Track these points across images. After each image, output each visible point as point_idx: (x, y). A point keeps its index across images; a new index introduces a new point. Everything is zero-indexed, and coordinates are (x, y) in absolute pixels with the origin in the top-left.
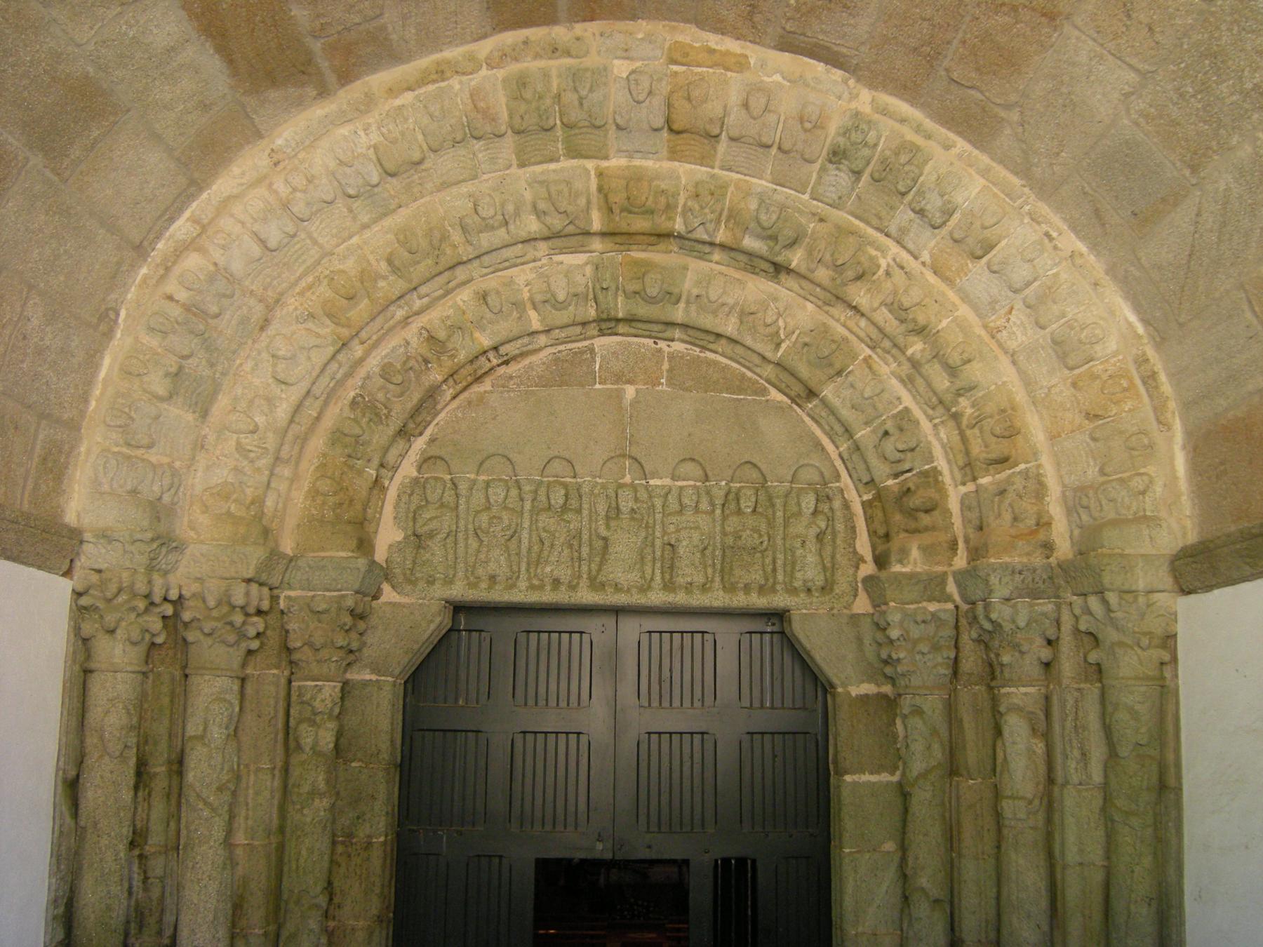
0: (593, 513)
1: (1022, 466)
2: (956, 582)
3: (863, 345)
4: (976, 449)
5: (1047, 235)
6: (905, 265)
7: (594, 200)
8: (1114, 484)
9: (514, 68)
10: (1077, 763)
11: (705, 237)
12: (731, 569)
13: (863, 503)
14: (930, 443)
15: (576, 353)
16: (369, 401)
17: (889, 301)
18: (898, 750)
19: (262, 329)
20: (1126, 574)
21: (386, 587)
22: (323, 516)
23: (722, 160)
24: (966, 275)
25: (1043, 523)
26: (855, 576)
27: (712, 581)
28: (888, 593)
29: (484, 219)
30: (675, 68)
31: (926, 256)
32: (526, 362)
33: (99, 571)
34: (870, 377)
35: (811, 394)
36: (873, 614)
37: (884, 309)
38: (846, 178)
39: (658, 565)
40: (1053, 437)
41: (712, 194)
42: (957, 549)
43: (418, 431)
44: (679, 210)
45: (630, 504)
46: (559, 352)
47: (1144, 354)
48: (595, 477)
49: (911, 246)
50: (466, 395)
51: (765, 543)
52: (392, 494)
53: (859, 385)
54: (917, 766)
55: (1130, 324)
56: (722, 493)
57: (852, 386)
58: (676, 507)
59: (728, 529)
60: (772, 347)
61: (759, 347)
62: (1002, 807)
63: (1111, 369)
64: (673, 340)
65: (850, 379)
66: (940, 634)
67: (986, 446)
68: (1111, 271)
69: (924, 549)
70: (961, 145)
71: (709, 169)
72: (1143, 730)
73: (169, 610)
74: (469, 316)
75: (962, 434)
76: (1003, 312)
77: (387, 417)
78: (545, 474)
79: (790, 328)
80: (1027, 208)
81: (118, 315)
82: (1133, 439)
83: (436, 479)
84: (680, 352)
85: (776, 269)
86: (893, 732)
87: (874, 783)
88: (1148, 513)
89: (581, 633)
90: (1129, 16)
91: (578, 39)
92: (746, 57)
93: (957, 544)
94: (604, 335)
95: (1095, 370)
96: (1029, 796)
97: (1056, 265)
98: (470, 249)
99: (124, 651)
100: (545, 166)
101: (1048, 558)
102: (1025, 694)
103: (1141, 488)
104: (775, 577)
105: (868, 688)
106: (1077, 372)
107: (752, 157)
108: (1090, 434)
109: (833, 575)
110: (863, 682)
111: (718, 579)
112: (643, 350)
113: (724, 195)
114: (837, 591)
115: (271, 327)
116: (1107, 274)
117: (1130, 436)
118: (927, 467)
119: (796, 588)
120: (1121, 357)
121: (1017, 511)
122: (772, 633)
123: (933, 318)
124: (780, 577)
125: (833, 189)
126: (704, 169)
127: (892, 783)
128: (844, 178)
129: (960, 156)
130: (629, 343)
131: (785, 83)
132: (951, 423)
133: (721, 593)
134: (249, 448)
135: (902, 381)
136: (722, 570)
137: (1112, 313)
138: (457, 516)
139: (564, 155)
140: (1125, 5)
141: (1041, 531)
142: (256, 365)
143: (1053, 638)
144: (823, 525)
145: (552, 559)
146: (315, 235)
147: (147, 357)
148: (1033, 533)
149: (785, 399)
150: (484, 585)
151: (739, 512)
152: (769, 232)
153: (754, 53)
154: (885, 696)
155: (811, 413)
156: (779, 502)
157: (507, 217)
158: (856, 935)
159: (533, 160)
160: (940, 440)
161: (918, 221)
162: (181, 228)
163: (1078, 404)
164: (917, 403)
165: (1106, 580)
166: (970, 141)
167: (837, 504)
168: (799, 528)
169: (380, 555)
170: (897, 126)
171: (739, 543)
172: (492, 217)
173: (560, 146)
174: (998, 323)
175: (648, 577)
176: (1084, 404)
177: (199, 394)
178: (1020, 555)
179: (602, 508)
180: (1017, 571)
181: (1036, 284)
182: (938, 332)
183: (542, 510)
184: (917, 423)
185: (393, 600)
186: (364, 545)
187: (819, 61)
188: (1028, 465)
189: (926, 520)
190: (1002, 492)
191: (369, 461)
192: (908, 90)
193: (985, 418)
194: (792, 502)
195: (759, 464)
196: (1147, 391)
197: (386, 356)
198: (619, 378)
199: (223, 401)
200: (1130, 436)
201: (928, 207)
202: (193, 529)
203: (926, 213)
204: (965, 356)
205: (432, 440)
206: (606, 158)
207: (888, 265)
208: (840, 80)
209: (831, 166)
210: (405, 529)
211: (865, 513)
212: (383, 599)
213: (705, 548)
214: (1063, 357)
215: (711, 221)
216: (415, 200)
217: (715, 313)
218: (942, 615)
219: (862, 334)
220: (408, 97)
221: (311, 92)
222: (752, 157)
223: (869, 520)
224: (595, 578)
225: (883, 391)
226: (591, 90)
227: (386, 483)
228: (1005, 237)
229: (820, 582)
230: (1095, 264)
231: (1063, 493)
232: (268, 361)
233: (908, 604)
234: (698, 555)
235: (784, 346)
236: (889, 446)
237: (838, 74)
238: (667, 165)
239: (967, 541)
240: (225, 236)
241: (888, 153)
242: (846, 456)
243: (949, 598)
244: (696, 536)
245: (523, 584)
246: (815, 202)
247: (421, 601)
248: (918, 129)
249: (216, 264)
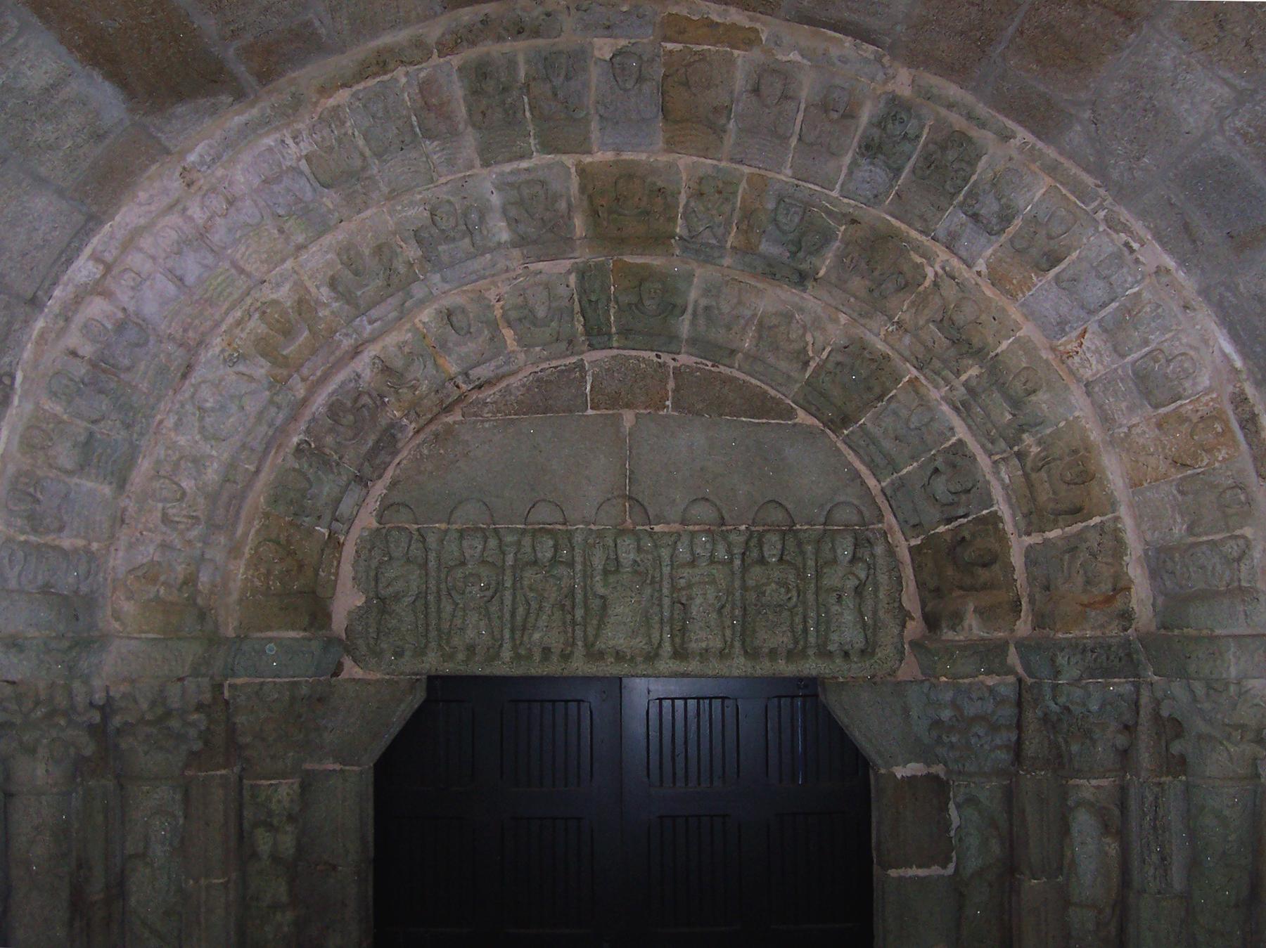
0: (587, 562)
1: (1097, 520)
3: (908, 365)
4: (1044, 496)
5: (1127, 244)
6: (957, 274)
8: (1204, 548)
9: (470, 54)
10: (1156, 869)
12: (754, 631)
13: (910, 549)
14: (988, 482)
15: (562, 371)
16: (316, 448)
17: (938, 317)
19: (184, 376)
20: (1215, 661)
21: (348, 662)
22: (269, 588)
24: (1030, 289)
25: (1121, 587)
26: (901, 635)
27: (732, 646)
29: (443, 231)
30: (670, 46)
31: (981, 265)
32: (503, 384)
33: (13, 683)
34: (916, 404)
35: (846, 421)
36: (922, 682)
37: (931, 325)
38: (883, 174)
39: (667, 629)
40: (1135, 485)
41: (720, 192)
43: (376, 474)
44: (681, 210)
45: (632, 556)
47: (1242, 392)
48: (588, 524)
49: (964, 254)
50: (433, 427)
51: (795, 599)
52: (349, 551)
53: (904, 413)
54: (973, 864)
55: (1225, 356)
56: (742, 539)
57: (895, 413)
58: (688, 557)
59: (751, 583)
61: (783, 365)
63: (1203, 410)
64: (678, 354)
65: (893, 405)
67: (1054, 493)
68: (1204, 292)
69: (979, 611)
70: (1023, 134)
71: (715, 162)
72: (1232, 837)
73: (97, 717)
75: (1026, 475)
76: (1075, 334)
77: (338, 464)
78: (528, 520)
79: (819, 345)
80: (1101, 214)
81: (13, 378)
82: (1229, 493)
83: (399, 529)
84: (688, 367)
85: (800, 274)
87: (925, 877)
88: (1244, 584)
89: (579, 701)
90: (1221, 28)
91: (548, 15)
92: (756, 31)
94: (595, 349)
95: (1183, 410)
97: (1137, 282)
99: (47, 771)
100: (515, 165)
101: (1125, 629)
102: (1098, 787)
103: (1235, 555)
104: (806, 639)
105: (914, 768)
106: (1162, 411)
108: (1178, 485)
109: (875, 635)
111: (737, 644)
113: (735, 193)
115: (195, 374)
116: (1199, 293)
117: (1224, 491)
118: (985, 512)
119: (831, 652)
120: (1214, 396)
121: (1090, 574)
122: (804, 696)
123: (990, 340)
124: (812, 640)
125: (867, 186)
126: (709, 161)
128: (881, 175)
129: (1021, 149)
130: (628, 358)
131: (805, 61)
132: (1015, 461)
133: (742, 660)
134: (177, 519)
135: (956, 409)
136: (743, 633)
137: (1206, 342)
138: (427, 575)
139: (537, 151)
140: (1216, 16)
141: (1118, 597)
142: (180, 419)
143: (1131, 723)
144: (863, 575)
145: (541, 623)
146: (241, 263)
147: (51, 426)
148: (1109, 600)
149: (816, 422)
150: (461, 656)
151: (762, 561)
153: (766, 28)
154: (936, 778)
155: (848, 441)
156: (809, 548)
160: (1001, 480)
161: (971, 225)
162: (84, 269)
163: (1164, 448)
164: (974, 435)
165: (1192, 668)
166: (1033, 133)
167: (879, 550)
168: (833, 578)
169: (339, 623)
170: (943, 112)
171: (764, 600)
172: (453, 228)
173: (532, 141)
174: (1069, 347)
175: (655, 641)
176: (1170, 449)
177: (115, 461)
178: (1093, 628)
179: (598, 560)
181: (1114, 305)
182: (997, 355)
183: (527, 564)
184: (973, 458)
185: (357, 677)
186: (318, 614)
187: (846, 35)
188: (1104, 518)
189: (984, 575)
190: (1073, 550)
191: (319, 517)
192: (954, 70)
193: (1054, 459)
194: (826, 547)
195: (784, 503)
196: (1245, 436)
197: (333, 393)
198: (615, 401)
199: (144, 465)
200: (1224, 491)
201: (982, 212)
202: (117, 619)
203: (980, 218)
204: (1029, 386)
205: (394, 484)
206: (589, 152)
207: (936, 274)
208: (872, 57)
209: (863, 161)
210: (366, 591)
211: (913, 560)
212: (344, 675)
213: (723, 607)
214: (1147, 394)
216: (359, 212)
217: (729, 328)
218: (1002, 690)
219: (907, 353)
220: (343, 96)
221: (226, 99)
223: (918, 569)
224: (593, 645)
225: (932, 419)
226: (568, 78)
227: (342, 539)
228: (1075, 250)
229: (859, 643)
230: (1187, 282)
231: (1146, 553)
232: (194, 414)
233: (962, 678)
234: (714, 615)
235: (813, 364)
236: (940, 487)
237: (869, 50)
238: (664, 158)
239: (1032, 601)
240: (133, 275)
241: (931, 147)
242: (889, 493)
243: (1011, 671)
244: (711, 592)
245: (506, 654)
246: (846, 200)
247: (387, 677)
248: (970, 117)
249: (124, 310)
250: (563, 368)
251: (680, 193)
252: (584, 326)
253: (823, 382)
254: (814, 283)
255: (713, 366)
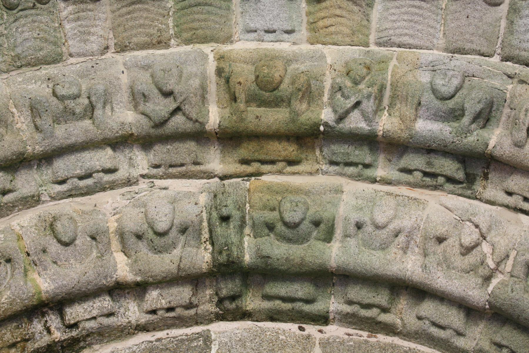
7: (212, 88)
11: (363, 126)
15: (182, 341)
23: (379, 31)
46: (159, 340)
60: (474, 280)
74: (27, 242)
79: (501, 249)
84: (338, 337)
98: (38, 136)
107: (416, 18)
112: (281, 337)
130: (263, 331)
152: (451, 104)
157: (93, 99)
159: (135, 40)
173: (171, 23)
206: (228, 39)
215: (369, 97)
222: (416, 18)
250: (184, 337)
251: (324, 75)
252: (212, 253)
253: (512, 292)
254: (484, 182)
255: (369, 337)
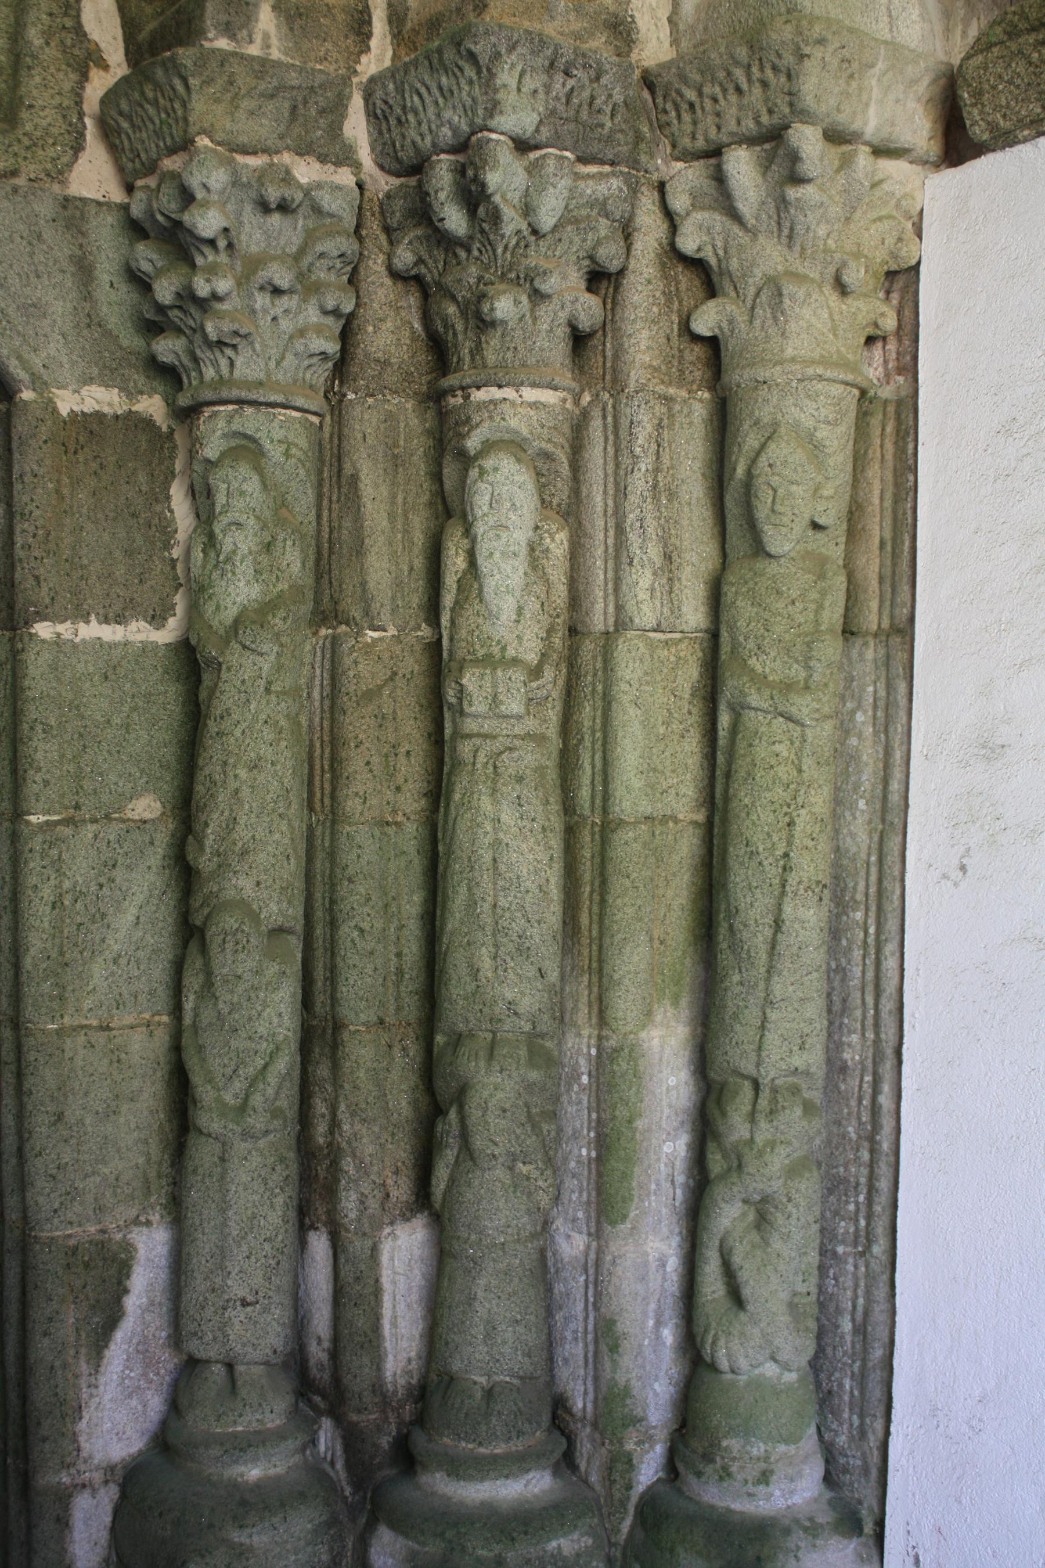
2: (372, 114)
18: (173, 562)
28: (198, 105)
36: (125, 208)
42: (369, 35)
62: (461, 690)
66: (319, 248)
86: (161, 516)
87: (112, 646)
93: (369, 23)
96: (532, 658)
102: (535, 405)
110: (88, 381)
114: (29, 127)
127: (155, 645)
143: (614, 266)
154: (147, 423)
158: (60, 1033)
180: (561, 62)
218: (328, 201)
233: (245, 151)
243: (346, 158)
